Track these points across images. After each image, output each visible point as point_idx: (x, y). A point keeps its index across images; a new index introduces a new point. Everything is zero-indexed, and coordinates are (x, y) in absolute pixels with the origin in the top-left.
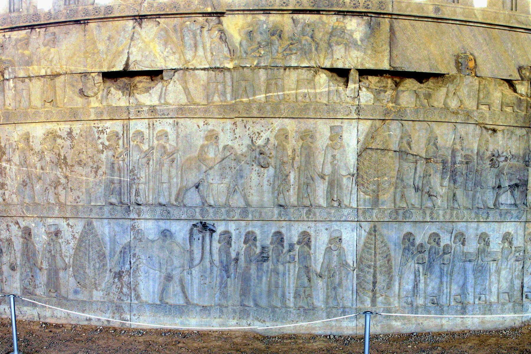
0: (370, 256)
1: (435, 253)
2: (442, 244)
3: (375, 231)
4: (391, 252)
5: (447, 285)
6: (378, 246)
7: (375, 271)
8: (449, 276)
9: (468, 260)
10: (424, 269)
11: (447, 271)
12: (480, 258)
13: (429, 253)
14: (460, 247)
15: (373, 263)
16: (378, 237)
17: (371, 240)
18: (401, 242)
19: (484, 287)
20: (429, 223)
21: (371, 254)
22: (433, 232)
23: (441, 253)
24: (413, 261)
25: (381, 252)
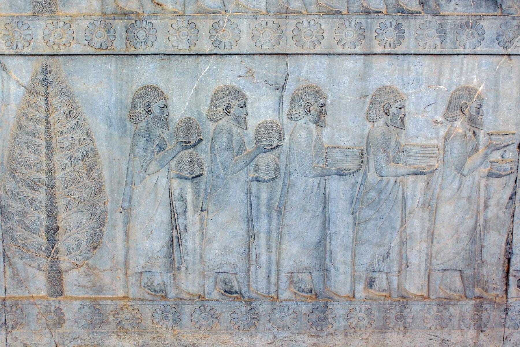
0: (33, 157)
1: (229, 148)
2: (253, 123)
3: (46, 83)
4: (97, 144)
5: (268, 241)
6: (55, 128)
7: (51, 198)
8: (275, 215)
9: (334, 169)
10: (197, 194)
11: (270, 199)
12: (372, 164)
13: (212, 148)
14: (309, 131)
15: (43, 177)
16: (54, 101)
17: (37, 109)
18: (127, 116)
19: (382, 251)
20: (212, 58)
21: (37, 151)
22: (222, 84)
23: (250, 148)
24: (164, 171)
25: (65, 143)
